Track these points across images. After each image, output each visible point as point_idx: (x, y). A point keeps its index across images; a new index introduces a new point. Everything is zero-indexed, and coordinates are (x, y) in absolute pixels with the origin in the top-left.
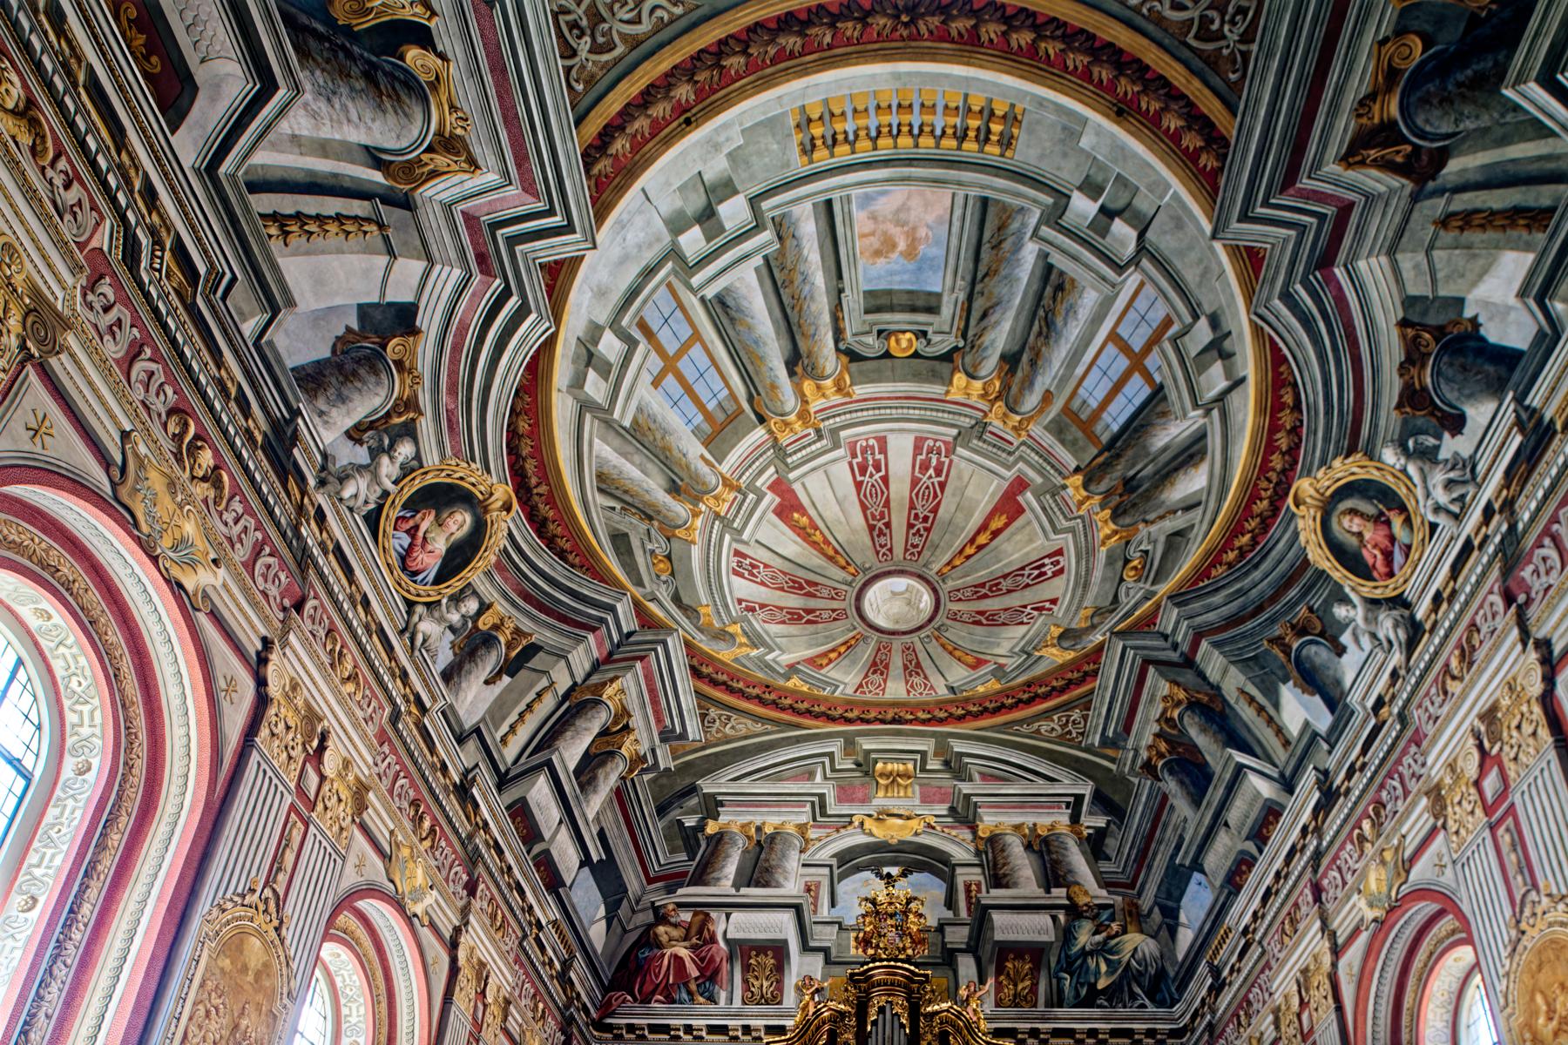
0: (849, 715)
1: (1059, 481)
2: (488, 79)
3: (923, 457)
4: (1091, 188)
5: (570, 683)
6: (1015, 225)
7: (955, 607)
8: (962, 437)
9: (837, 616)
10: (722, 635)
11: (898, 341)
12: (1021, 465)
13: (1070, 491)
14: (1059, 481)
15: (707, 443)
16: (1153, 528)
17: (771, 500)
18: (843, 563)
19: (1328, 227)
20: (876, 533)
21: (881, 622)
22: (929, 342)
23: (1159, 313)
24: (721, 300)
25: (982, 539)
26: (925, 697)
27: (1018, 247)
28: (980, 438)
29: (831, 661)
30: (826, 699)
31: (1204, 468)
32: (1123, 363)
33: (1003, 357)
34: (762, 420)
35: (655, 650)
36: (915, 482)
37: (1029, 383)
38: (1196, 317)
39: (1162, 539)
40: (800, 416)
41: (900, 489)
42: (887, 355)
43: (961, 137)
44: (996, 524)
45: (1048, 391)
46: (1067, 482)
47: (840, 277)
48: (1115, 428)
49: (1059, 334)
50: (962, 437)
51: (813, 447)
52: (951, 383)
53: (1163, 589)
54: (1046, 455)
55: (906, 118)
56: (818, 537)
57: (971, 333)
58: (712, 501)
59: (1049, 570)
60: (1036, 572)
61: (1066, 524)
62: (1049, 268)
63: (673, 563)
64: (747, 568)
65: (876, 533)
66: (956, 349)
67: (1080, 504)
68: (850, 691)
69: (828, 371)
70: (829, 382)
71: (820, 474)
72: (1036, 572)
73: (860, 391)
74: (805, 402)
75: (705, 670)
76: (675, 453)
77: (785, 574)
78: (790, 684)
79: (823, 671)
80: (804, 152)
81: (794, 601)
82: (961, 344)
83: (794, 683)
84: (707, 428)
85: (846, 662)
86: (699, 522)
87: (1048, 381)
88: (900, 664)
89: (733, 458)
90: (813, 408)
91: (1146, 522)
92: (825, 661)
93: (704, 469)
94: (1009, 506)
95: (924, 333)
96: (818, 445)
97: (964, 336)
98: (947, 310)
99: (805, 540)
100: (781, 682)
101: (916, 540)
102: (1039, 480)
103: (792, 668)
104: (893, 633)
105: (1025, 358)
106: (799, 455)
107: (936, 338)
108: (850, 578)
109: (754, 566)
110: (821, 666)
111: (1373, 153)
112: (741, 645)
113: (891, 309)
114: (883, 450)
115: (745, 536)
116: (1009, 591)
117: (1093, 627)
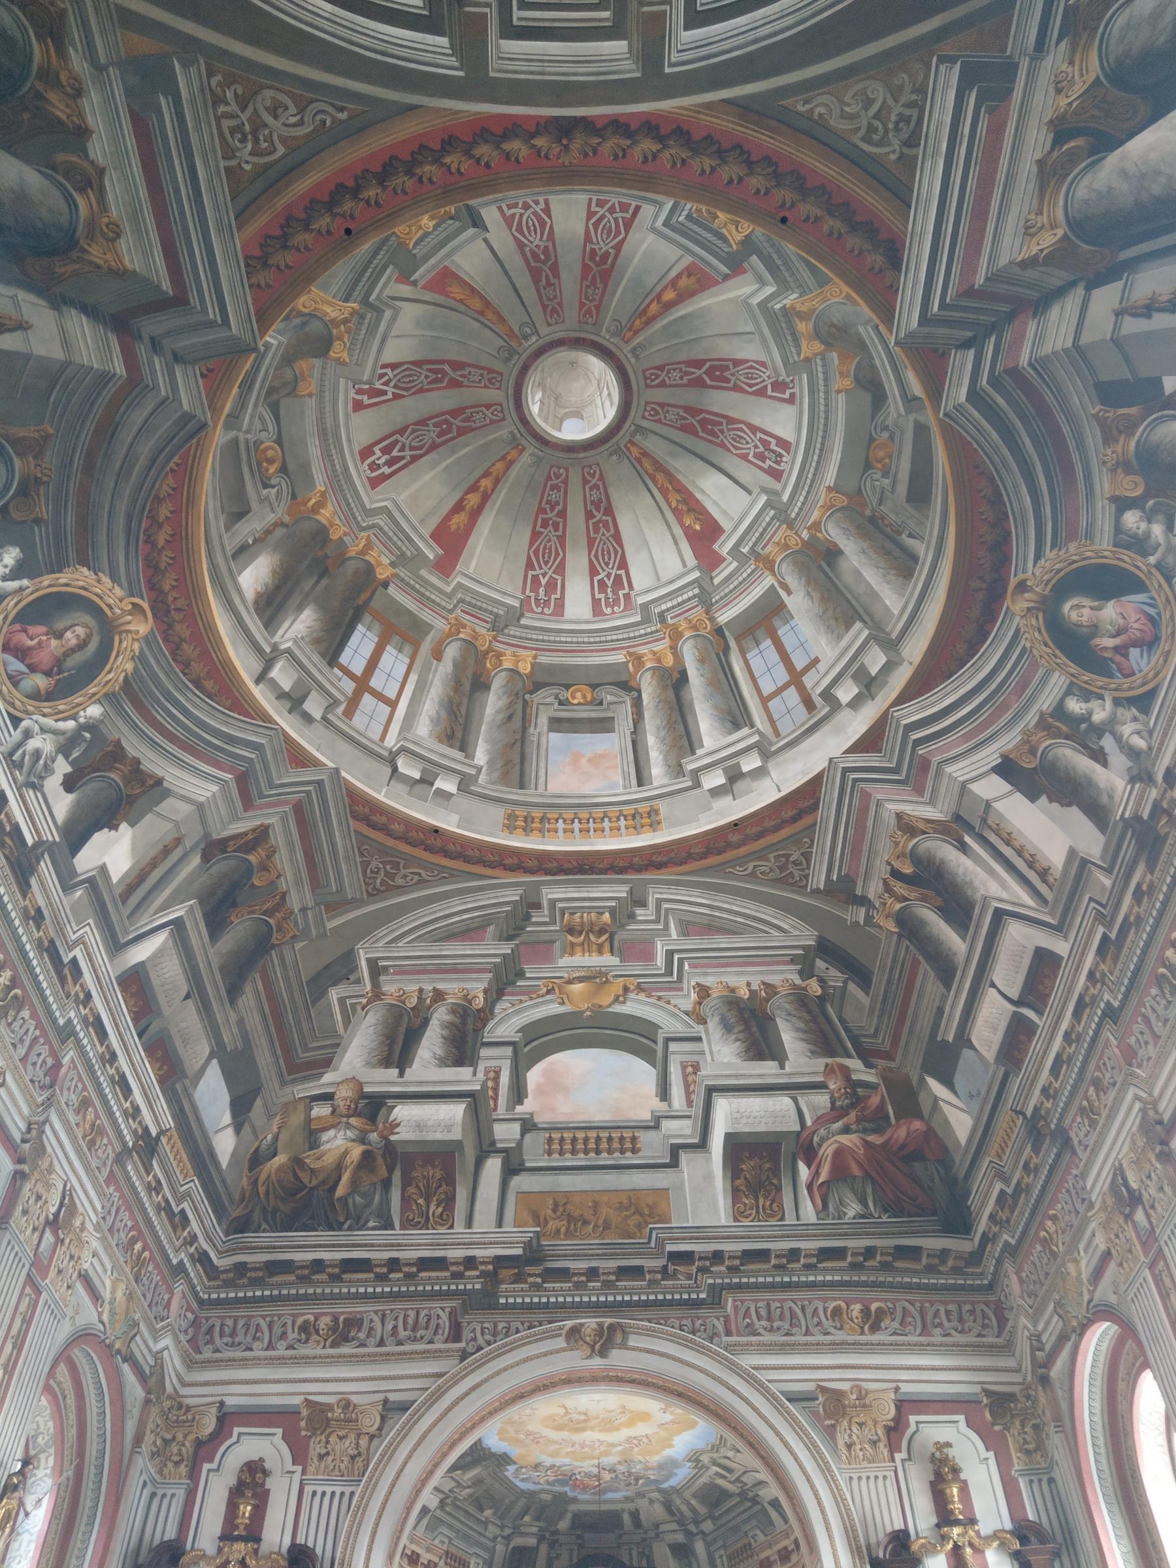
0: (648, 145)
1: (402, 572)
2: (866, 848)
5: (1097, 293)
6: (496, 775)
7: (493, 395)
8: (514, 616)
9: (656, 376)
10: (835, 335)
11: (584, 697)
12: (449, 590)
13: (385, 561)
14: (402, 572)
15: (782, 606)
16: (271, 518)
17: (724, 547)
18: (646, 462)
19: (254, 792)
21: (596, 365)
22: (556, 697)
23: (359, 721)
24: (736, 726)
25: (473, 500)
26: (520, 195)
27: (491, 762)
28: (497, 616)
29: (674, 283)
30: (689, 191)
31: (250, 595)
32: (376, 682)
33: (488, 687)
34: (719, 631)
35: (943, 305)
36: (561, 569)
37: (458, 666)
38: (324, 718)
39: (254, 505)
40: (681, 635)
41: (577, 562)
42: (594, 687)
43: (542, 820)
44: (460, 519)
45: (439, 660)
46: (391, 570)
47: (634, 743)
48: (360, 627)
49: (441, 704)
50: (514, 616)
51: (669, 604)
52: (533, 665)
53: (219, 437)
54: (423, 600)
55: (584, 826)
56: (674, 498)
57: (520, 705)
58: (792, 543)
59: (378, 456)
60: (395, 453)
61: (377, 520)
62: (462, 749)
63: (865, 457)
64: (769, 454)
66: (531, 692)
67: (369, 546)
68: (647, 210)
69: (648, 675)
70: (649, 665)
71: (665, 576)
72: (395, 453)
73: (619, 657)
74: (673, 648)
75: (876, 259)
76: (817, 595)
77: (722, 446)
78: (746, 228)
79: (688, 260)
80: (657, 812)
81: (721, 401)
82: (527, 696)
83: (737, 231)
84: (776, 622)
85: (650, 281)
86: (815, 515)
87: (440, 668)
88: (564, 275)
89: (756, 592)
90: (666, 642)
91: (283, 524)
92: (684, 282)
93: (792, 580)
94: (451, 540)
95: (561, 703)
96: (664, 607)
98: (543, 721)
99: (691, 495)
100: (759, 232)
101: (554, 496)
102: (424, 573)
103: (736, 265)
104: (578, 343)
105: (467, 687)
106: (685, 597)
107: (550, 700)
108: (638, 438)
109: (761, 457)
110: (690, 271)
111: (250, 837)
112: (803, 316)
113: (591, 720)
114: (596, 603)
115: (764, 499)
116: (422, 422)
117: (288, 360)
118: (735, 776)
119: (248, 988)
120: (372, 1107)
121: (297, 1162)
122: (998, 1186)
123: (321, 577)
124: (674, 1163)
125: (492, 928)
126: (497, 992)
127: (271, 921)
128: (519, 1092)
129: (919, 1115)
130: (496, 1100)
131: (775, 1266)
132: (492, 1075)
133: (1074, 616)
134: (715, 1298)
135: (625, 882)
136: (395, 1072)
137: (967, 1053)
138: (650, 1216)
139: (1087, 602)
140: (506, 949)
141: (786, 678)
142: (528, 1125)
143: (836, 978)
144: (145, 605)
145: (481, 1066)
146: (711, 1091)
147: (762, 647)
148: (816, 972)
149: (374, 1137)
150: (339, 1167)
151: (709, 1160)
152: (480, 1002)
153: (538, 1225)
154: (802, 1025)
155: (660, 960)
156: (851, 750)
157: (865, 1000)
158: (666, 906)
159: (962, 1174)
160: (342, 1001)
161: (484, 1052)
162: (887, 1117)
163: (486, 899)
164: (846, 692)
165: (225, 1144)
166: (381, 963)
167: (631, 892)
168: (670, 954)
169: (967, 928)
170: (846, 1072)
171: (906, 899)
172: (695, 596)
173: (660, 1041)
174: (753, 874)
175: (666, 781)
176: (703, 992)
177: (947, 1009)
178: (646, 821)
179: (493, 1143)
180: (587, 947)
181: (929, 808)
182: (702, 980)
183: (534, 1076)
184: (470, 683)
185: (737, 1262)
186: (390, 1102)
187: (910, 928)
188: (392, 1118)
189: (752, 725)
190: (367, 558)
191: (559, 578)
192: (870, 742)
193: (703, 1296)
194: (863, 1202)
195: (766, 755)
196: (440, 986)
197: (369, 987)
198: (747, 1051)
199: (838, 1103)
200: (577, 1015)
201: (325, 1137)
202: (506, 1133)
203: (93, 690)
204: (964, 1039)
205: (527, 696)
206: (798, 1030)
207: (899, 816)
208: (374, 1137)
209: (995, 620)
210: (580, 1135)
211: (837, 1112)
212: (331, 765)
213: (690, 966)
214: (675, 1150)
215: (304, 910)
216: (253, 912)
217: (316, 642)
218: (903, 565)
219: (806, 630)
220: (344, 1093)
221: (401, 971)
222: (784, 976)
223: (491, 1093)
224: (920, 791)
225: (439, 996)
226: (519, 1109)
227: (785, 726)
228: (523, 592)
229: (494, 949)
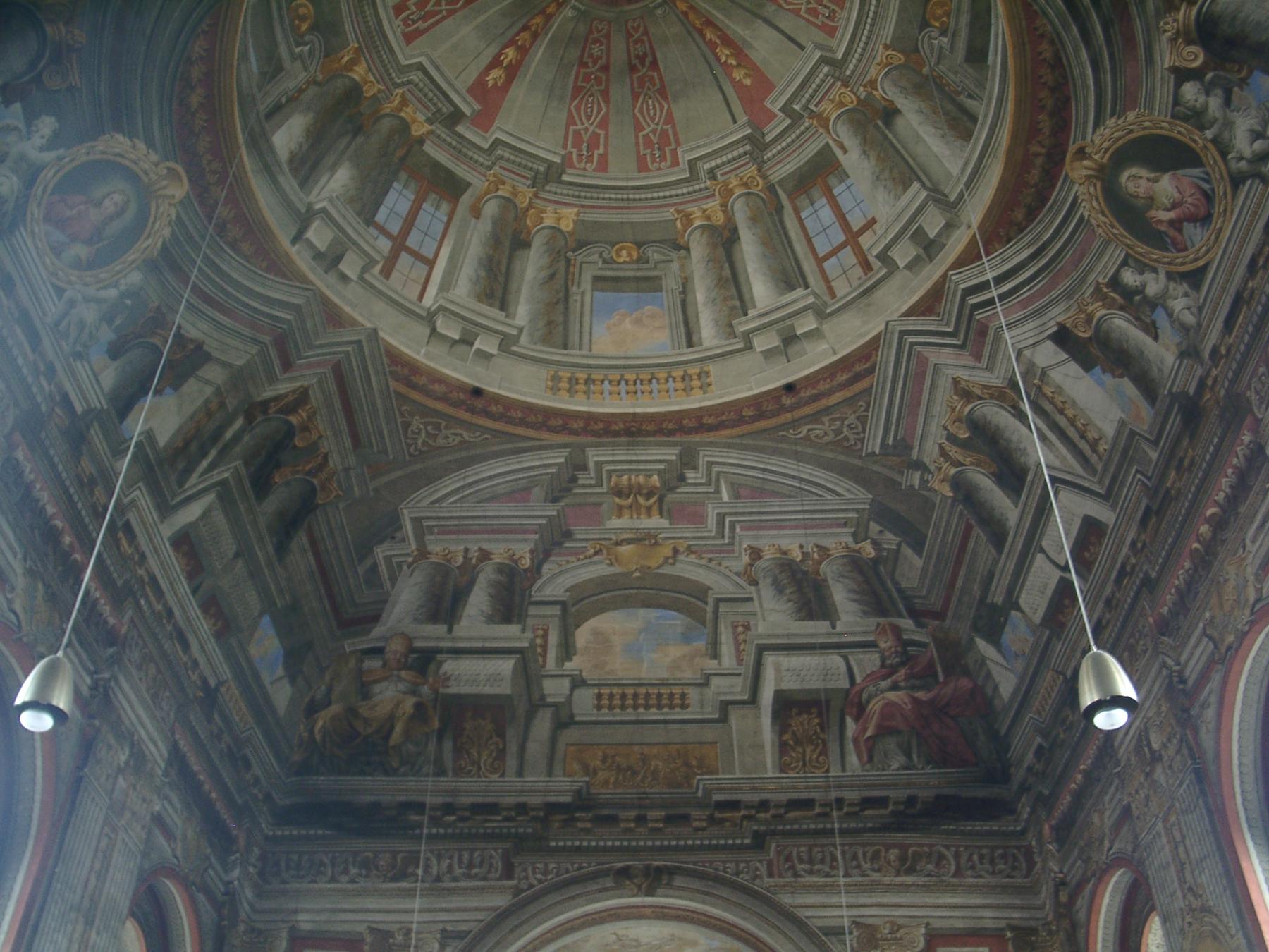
3: (596, 152)
4: (484, 356)
11: (630, 255)
17: (775, 104)
20: (649, 59)
22: (601, 255)
24: (792, 288)
28: (537, 172)
32: (412, 242)
34: (771, 188)
37: (499, 223)
38: (361, 278)
40: (731, 192)
42: (639, 245)
43: (586, 382)
45: (478, 218)
46: (427, 127)
47: (684, 304)
51: (719, 161)
52: (575, 222)
54: (459, 154)
57: (562, 263)
62: (503, 307)
65: (649, 59)
67: (404, 102)
69: (697, 234)
70: (697, 223)
74: (724, 205)
80: (707, 373)
82: (570, 254)
84: (832, 180)
91: (315, 82)
94: (489, 99)
95: (605, 262)
96: (713, 164)
97: (568, 261)
98: (587, 277)
106: (735, 153)
107: (596, 257)
118: (790, 339)
119: (294, 546)
120: (423, 661)
121: (352, 711)
122: (1039, 740)
123: (355, 135)
124: (724, 719)
125: (537, 489)
126: (543, 554)
127: (315, 481)
128: (567, 650)
129: (966, 672)
130: (544, 655)
131: (819, 815)
132: (541, 632)
133: (1131, 187)
134: (759, 842)
135: (675, 444)
136: (444, 628)
137: (1014, 614)
138: (700, 767)
139: (1144, 173)
140: (552, 511)
141: (842, 238)
142: (578, 682)
143: (891, 540)
144: (180, 169)
145: (530, 622)
146: (762, 649)
147: (817, 205)
148: (870, 534)
149: (425, 689)
150: (391, 719)
151: (758, 717)
152: (526, 562)
153: (587, 774)
154: (855, 587)
155: (711, 521)
156: (908, 313)
157: (918, 562)
158: (716, 469)
159: (1003, 731)
160: (388, 559)
161: (532, 610)
162: (935, 675)
163: (529, 461)
164: (903, 254)
165: (282, 695)
166: (426, 523)
167: (680, 456)
168: (721, 518)
169: (1019, 495)
170: (897, 631)
171: (963, 465)
172: (746, 153)
173: (710, 601)
174: (807, 438)
175: (716, 342)
176: (756, 554)
177: (998, 572)
178: (696, 383)
179: (543, 697)
180: (634, 508)
181: (987, 374)
182: (754, 543)
183: (582, 636)
184: (510, 239)
185: (782, 811)
186: (439, 657)
187: (966, 494)
188: (442, 671)
189: (807, 287)
190: (402, 114)
191: (602, 133)
192: (928, 305)
193: (747, 841)
194: (908, 755)
195: (821, 315)
196: (485, 546)
197: (414, 546)
198: (799, 610)
199: (889, 662)
200: (627, 575)
201: (377, 688)
202: (555, 689)
203: (132, 257)
204: (1012, 603)
205: (570, 254)
206: (850, 591)
207: (956, 381)
208: (425, 689)
209: (1053, 187)
210: (630, 691)
211: (888, 670)
212: (369, 325)
213: (742, 529)
214: (725, 706)
215: (347, 470)
216: (297, 472)
217: (351, 201)
218: (960, 123)
219: (863, 190)
220: (396, 647)
221: (444, 531)
222: (838, 541)
223: (539, 650)
224: (978, 356)
225: (485, 556)
226: (568, 665)
227: (841, 288)
228: (565, 147)
229: (541, 511)
